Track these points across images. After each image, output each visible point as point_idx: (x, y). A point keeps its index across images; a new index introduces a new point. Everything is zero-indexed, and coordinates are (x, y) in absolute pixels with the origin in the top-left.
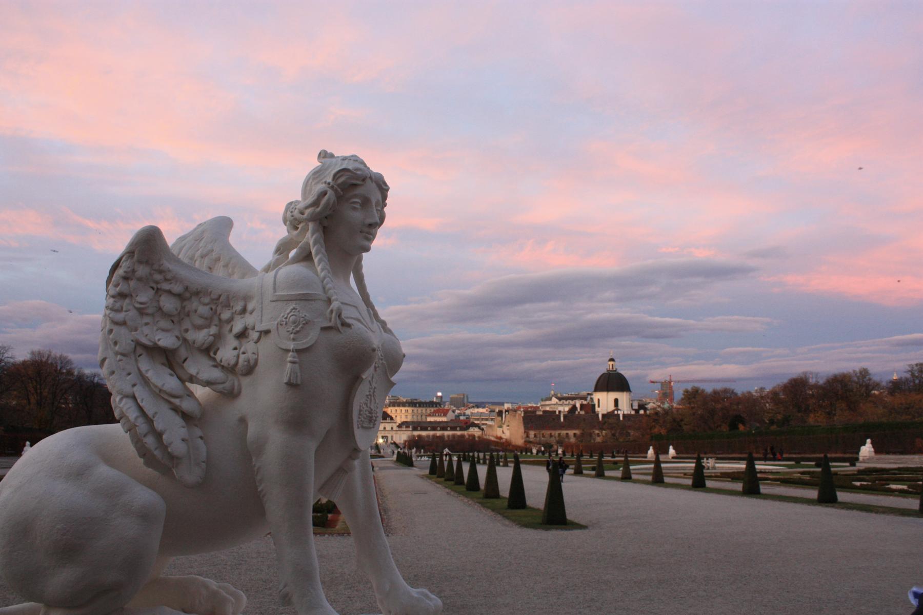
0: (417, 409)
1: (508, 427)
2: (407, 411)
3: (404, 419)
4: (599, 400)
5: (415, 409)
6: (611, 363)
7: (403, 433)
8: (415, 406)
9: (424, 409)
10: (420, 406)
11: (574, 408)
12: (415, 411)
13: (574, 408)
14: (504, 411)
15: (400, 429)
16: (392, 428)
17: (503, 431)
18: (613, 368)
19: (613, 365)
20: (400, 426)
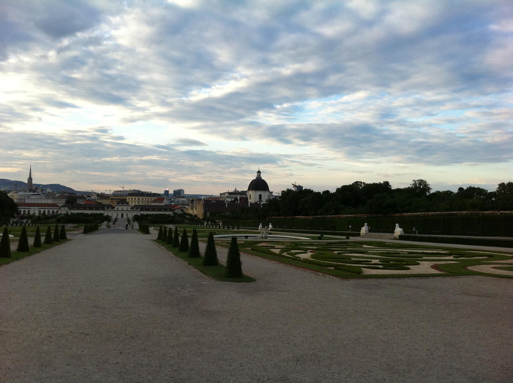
0: (146, 198)
1: (196, 210)
2: (139, 199)
3: (137, 204)
5: (144, 198)
8: (144, 196)
9: (150, 198)
10: (147, 196)
11: (236, 199)
13: (236, 199)
14: (195, 200)
15: (133, 210)
17: (193, 212)
18: (259, 177)
19: (259, 175)
20: (132, 208)
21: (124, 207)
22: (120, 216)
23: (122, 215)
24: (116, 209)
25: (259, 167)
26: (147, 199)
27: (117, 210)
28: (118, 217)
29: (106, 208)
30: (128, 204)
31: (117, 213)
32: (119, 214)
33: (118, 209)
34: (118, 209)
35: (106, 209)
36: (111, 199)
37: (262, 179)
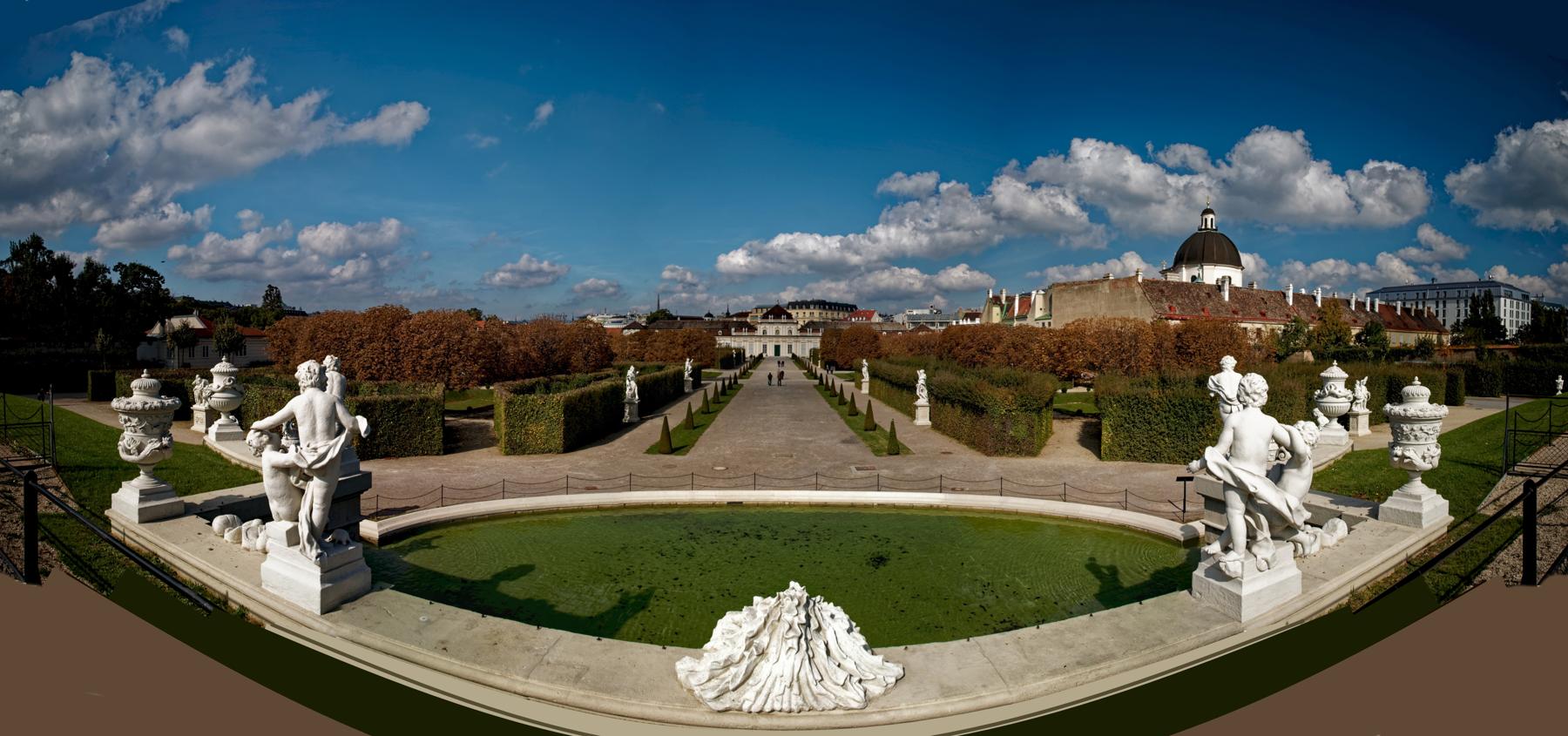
7: (808, 341)
15: (804, 334)
16: (790, 331)
20: (803, 329)
21: (780, 327)
22: (771, 352)
23: (777, 348)
24: (759, 332)
27: (762, 334)
28: (764, 355)
29: (733, 329)
30: (792, 318)
31: (762, 344)
32: (768, 347)
33: (764, 332)
34: (764, 332)
35: (734, 334)
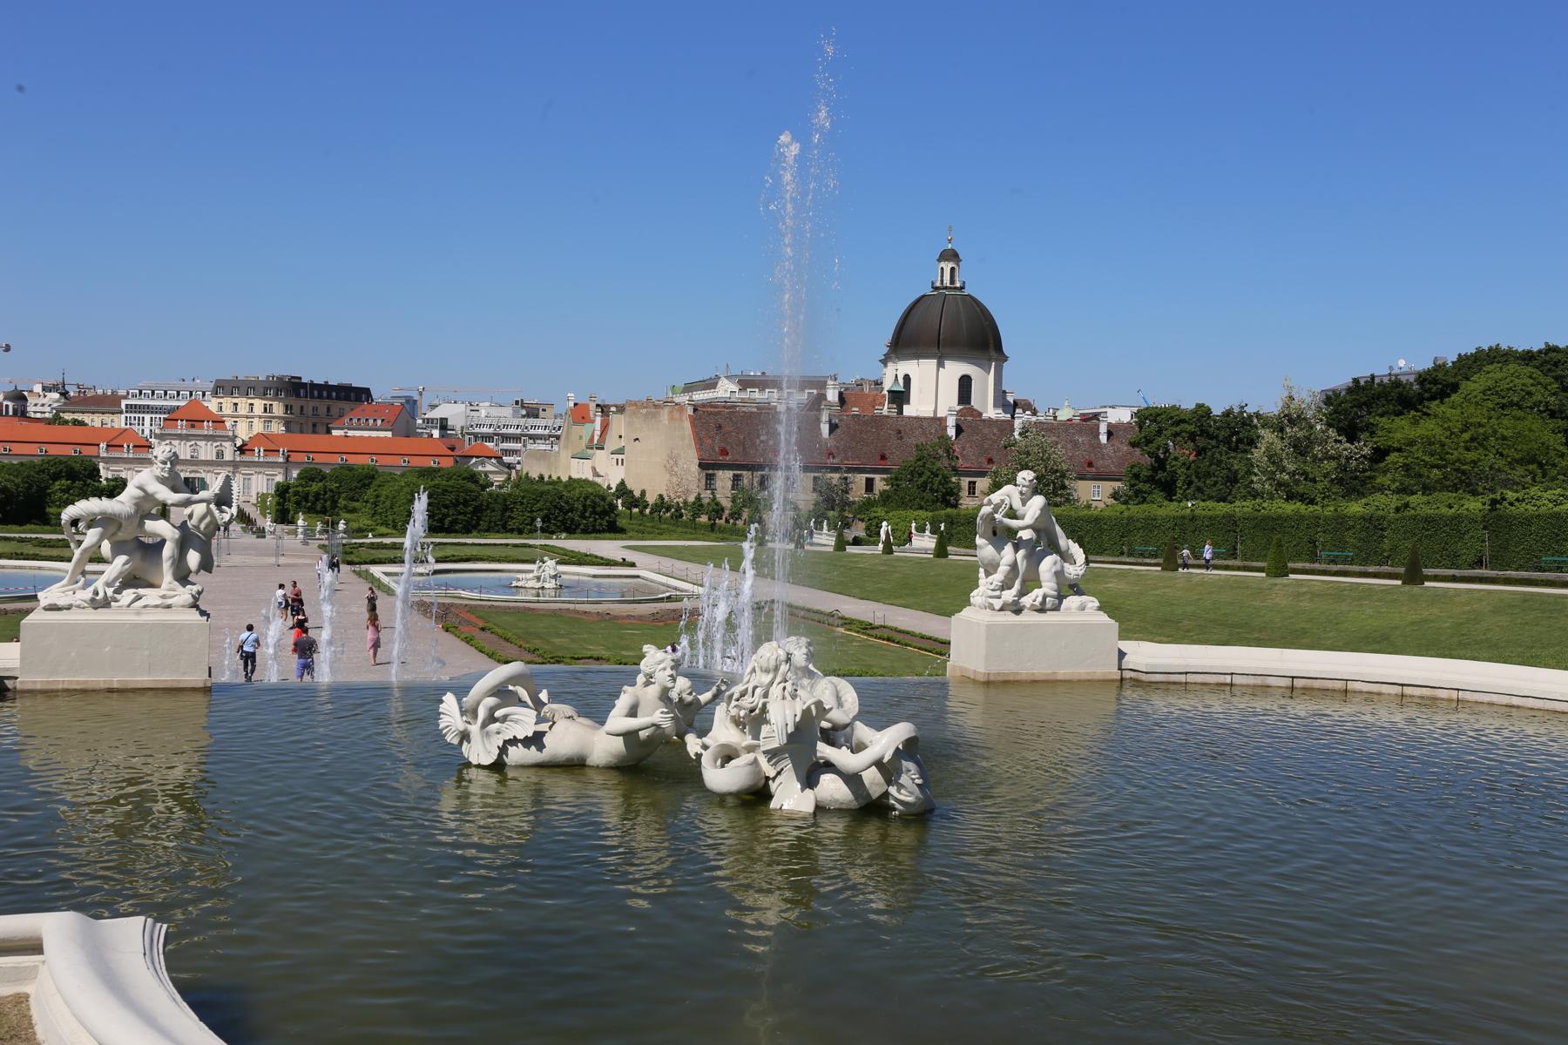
1: (620, 457)
4: (907, 379)
5: (296, 403)
6: (947, 266)
8: (298, 395)
12: (296, 410)
16: (220, 454)
17: (594, 469)
18: (952, 281)
19: (953, 269)
21: (202, 443)
25: (950, 229)
26: (311, 409)
36: (130, 408)
37: (968, 295)
